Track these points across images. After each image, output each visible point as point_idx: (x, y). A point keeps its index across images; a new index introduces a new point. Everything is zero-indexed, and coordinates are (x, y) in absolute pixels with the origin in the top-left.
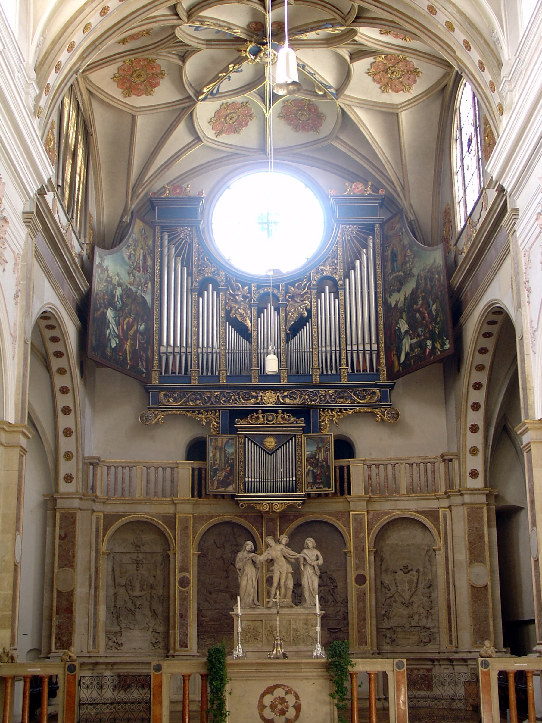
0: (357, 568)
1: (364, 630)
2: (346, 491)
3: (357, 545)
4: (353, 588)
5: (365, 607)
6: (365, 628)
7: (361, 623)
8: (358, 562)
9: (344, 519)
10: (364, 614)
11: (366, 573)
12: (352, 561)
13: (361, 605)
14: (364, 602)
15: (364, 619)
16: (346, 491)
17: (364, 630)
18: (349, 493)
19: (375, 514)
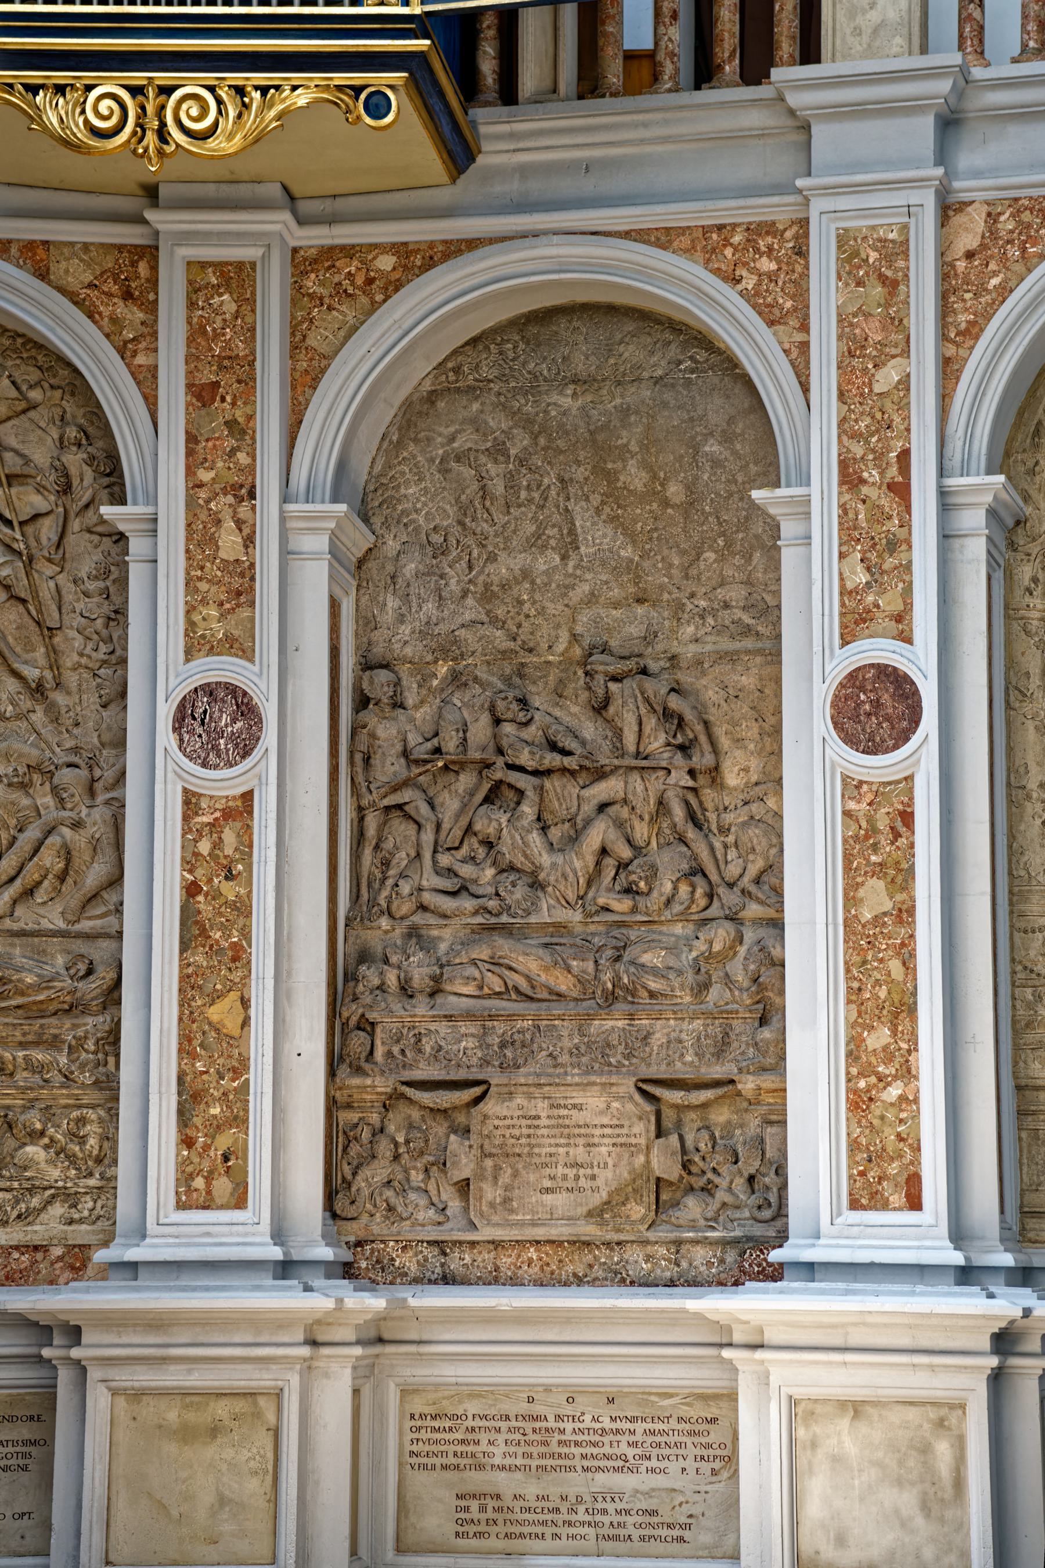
0: (855, 622)
1: (894, 1092)
2: (786, 45)
3: (858, 449)
4: (814, 770)
5: (905, 914)
6: (908, 1073)
7: (879, 1038)
8: (863, 578)
9: (767, 265)
10: (895, 967)
11: (919, 661)
12: (812, 577)
13: (876, 897)
14: (901, 877)
15: (904, 1008)
16: (786, 45)
17: (894, 1092)
18: (810, 51)
19: (1006, 224)
